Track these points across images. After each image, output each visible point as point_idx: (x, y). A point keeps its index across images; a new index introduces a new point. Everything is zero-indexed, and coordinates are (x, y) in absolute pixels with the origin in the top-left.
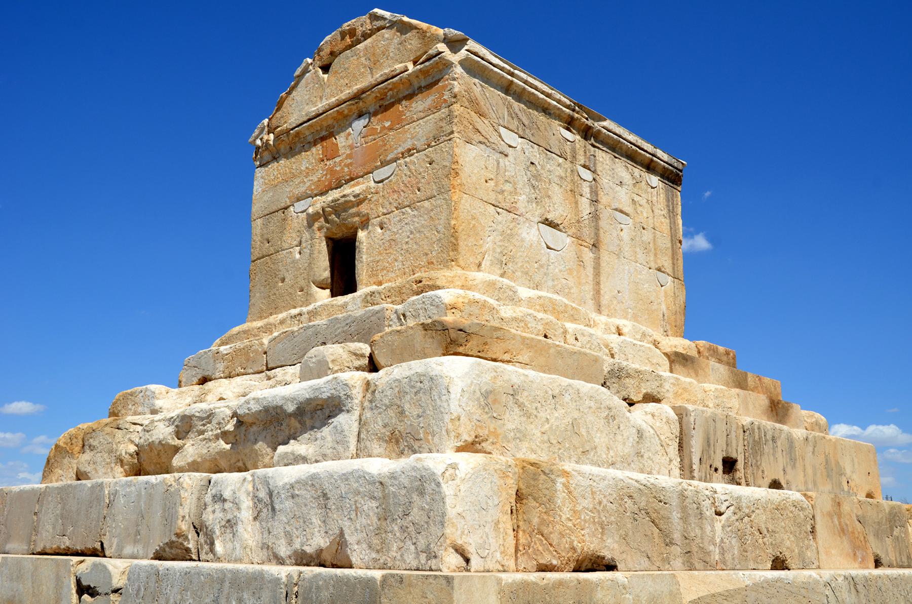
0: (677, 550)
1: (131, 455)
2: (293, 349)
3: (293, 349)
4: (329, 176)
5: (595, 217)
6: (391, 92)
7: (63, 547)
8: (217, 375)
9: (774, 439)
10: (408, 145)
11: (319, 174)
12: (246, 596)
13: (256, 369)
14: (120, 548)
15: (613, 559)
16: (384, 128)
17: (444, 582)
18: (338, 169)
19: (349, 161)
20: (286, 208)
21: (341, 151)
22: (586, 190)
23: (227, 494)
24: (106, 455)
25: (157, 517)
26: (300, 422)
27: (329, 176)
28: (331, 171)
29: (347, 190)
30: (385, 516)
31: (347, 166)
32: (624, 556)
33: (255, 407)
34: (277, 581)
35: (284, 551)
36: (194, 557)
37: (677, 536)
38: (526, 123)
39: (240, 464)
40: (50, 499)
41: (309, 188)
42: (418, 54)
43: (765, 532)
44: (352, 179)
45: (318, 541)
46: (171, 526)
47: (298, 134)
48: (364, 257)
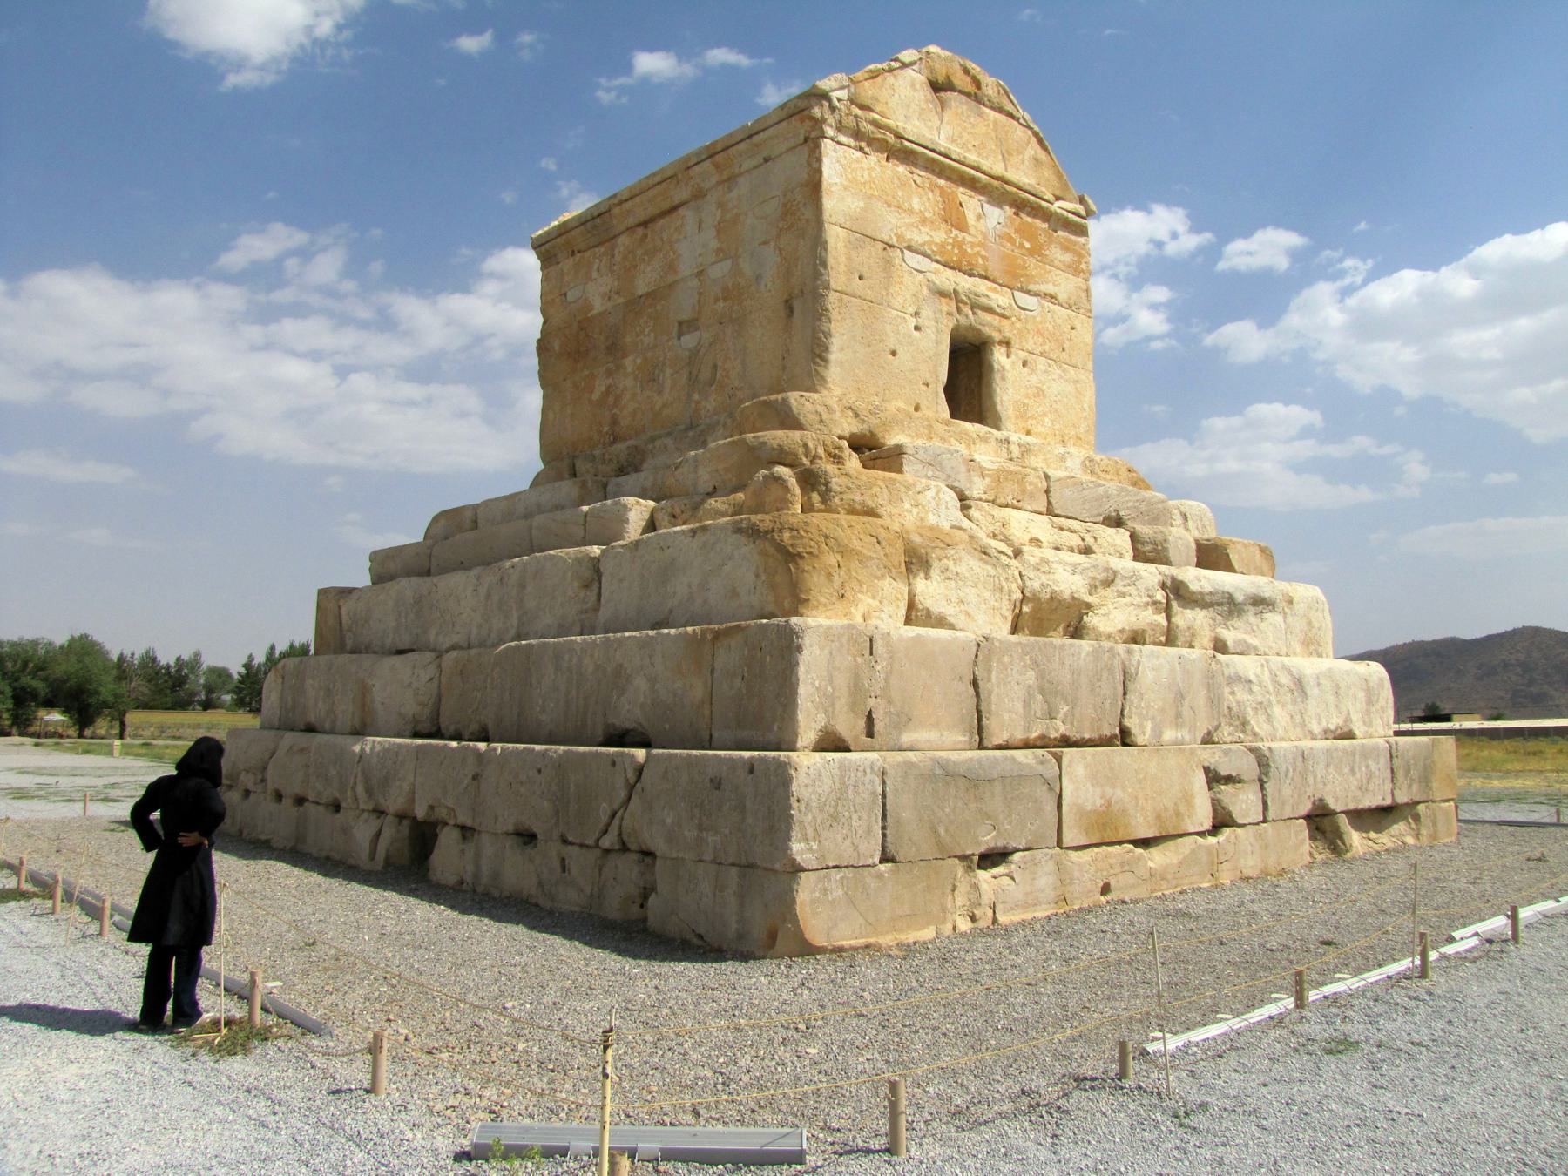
7: (1053, 735)
10: (1049, 288)
11: (940, 236)
14: (1158, 732)
16: (1022, 246)
20: (891, 246)
21: (972, 230)
23: (1252, 678)
24: (987, 595)
25: (1201, 700)
28: (958, 244)
29: (982, 286)
30: (1369, 702)
31: (984, 258)
33: (1207, 588)
35: (1316, 729)
40: (1006, 659)
42: (1058, 193)
44: (987, 278)
45: (1335, 722)
47: (912, 152)
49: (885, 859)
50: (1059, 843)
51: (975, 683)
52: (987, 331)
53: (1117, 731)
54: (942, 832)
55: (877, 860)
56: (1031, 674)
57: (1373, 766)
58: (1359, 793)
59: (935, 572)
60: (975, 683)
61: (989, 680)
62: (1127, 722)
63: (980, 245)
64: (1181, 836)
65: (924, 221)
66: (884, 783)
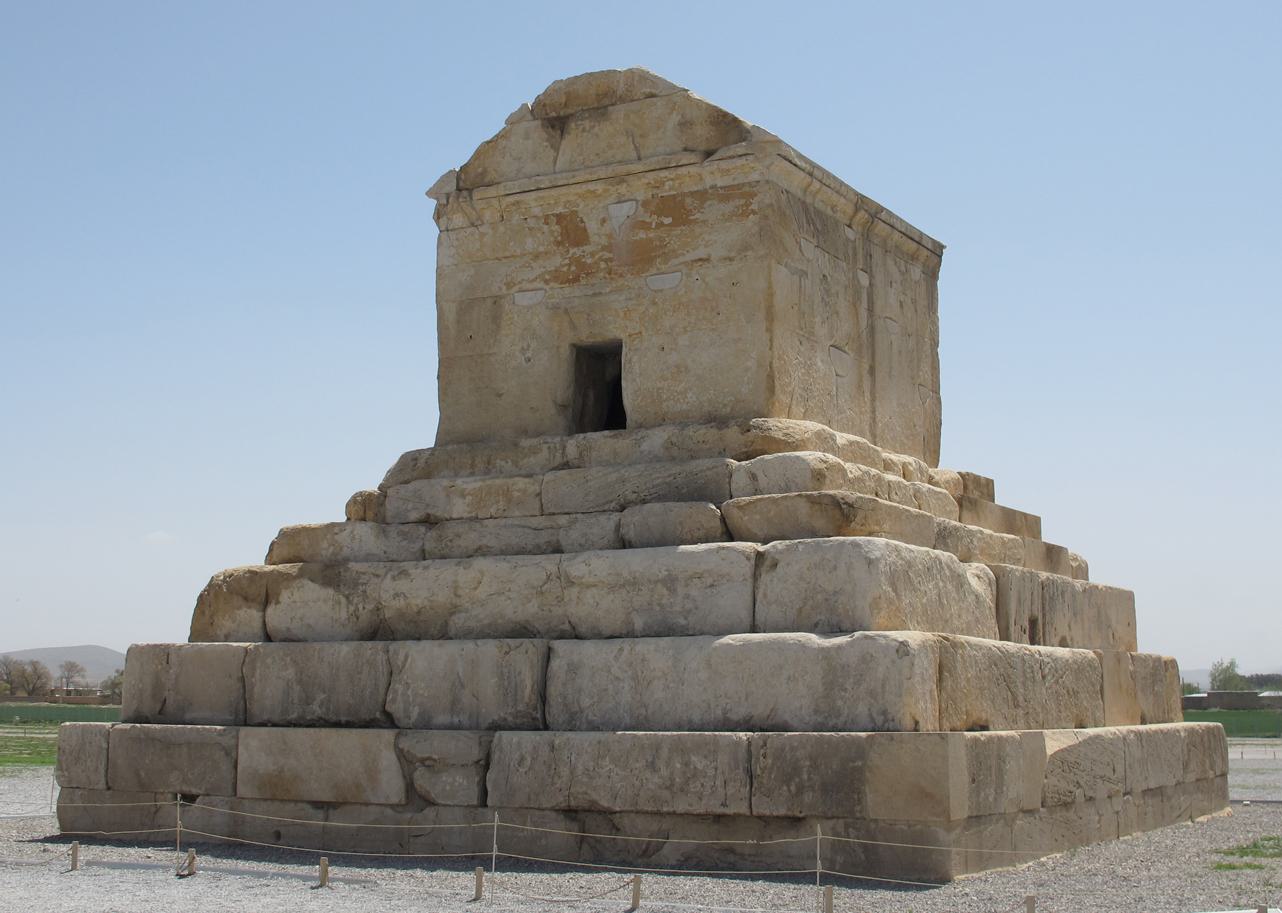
0: (1021, 712)
1: (371, 611)
2: (587, 495)
3: (587, 495)
4: (573, 268)
5: (872, 329)
6: (671, 182)
8: (454, 516)
9: (1063, 593)
10: (701, 253)
11: (557, 261)
12: (694, 758)
13: (527, 514)
15: (987, 720)
16: (660, 225)
17: (938, 738)
18: (589, 261)
19: (607, 255)
21: (594, 239)
22: (864, 297)
26: (668, 589)
27: (573, 268)
28: (577, 261)
31: (606, 261)
32: (993, 719)
34: (738, 743)
36: (541, 727)
37: (1021, 699)
38: (820, 228)
39: (566, 627)
40: (269, 661)
41: (540, 277)
43: (1071, 693)
44: (612, 279)
46: (516, 695)
48: (638, 380)
49: (109, 789)
50: (235, 795)
51: (242, 679)
52: (613, 330)
53: (378, 715)
54: (143, 774)
55: (102, 785)
56: (290, 673)
57: (698, 762)
58: (666, 794)
59: (285, 596)
60: (242, 679)
61: (253, 676)
62: (388, 708)
63: (604, 248)
64: (367, 804)
65: (537, 257)
66: (108, 743)
